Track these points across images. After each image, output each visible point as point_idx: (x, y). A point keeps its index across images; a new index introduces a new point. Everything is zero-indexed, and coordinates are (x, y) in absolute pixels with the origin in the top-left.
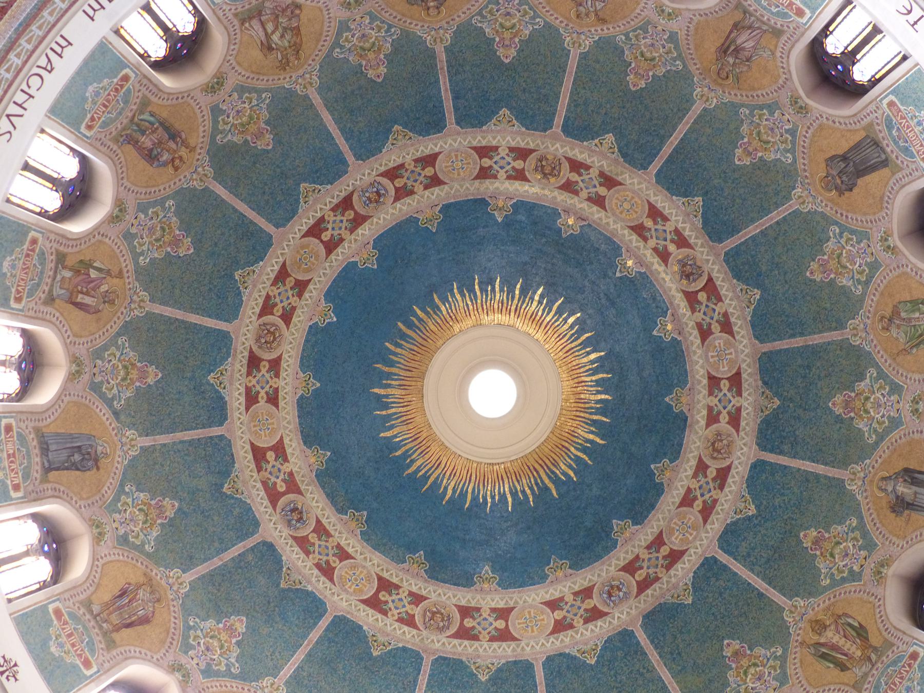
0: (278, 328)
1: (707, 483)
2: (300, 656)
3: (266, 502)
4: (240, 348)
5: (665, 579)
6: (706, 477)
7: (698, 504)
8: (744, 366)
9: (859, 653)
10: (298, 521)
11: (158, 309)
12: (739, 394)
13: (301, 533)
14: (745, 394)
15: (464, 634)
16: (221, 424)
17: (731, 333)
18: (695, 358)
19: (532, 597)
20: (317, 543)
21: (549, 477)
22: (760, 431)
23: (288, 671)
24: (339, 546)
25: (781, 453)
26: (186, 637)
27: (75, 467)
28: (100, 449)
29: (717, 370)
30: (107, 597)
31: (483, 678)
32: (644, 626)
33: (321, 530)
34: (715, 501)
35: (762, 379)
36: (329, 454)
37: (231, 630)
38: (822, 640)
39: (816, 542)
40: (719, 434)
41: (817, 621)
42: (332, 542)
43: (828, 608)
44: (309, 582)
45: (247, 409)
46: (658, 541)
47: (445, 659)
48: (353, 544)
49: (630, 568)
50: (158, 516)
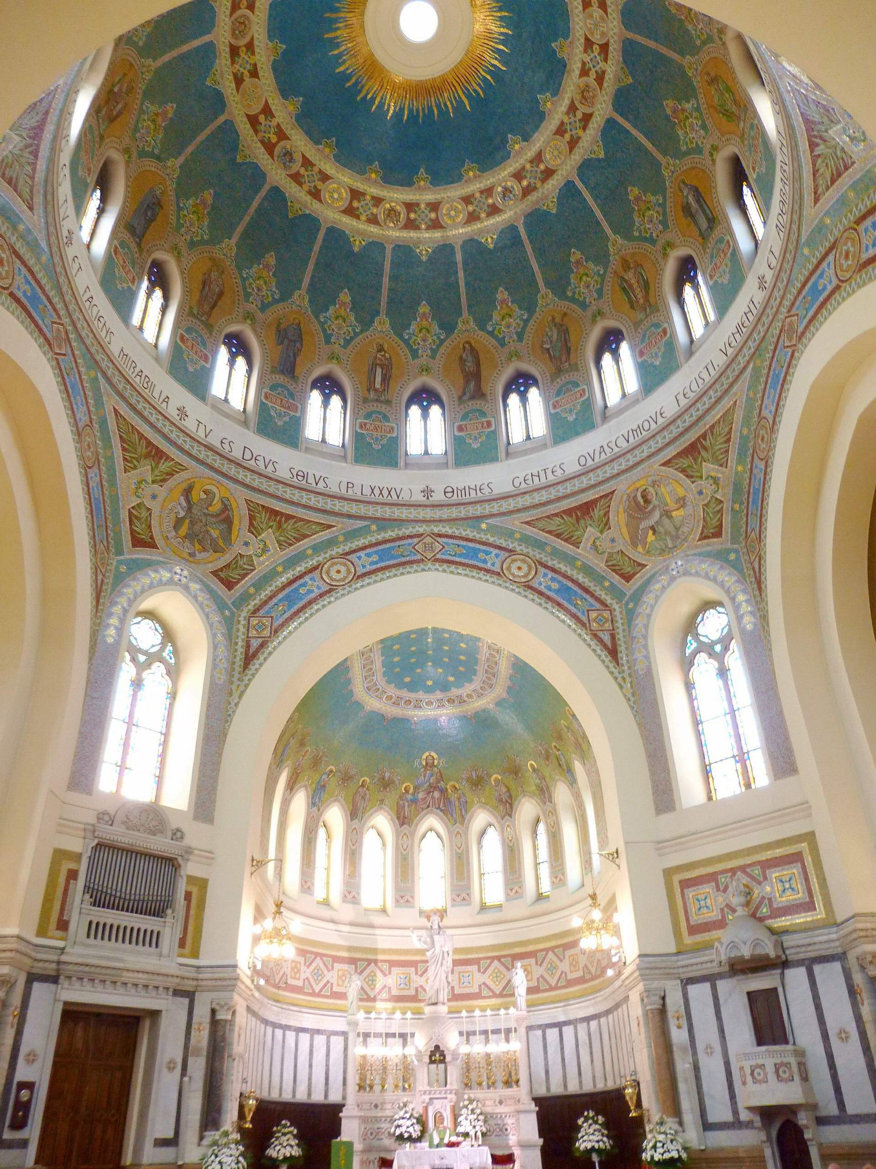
0: (248, 18)
1: (575, 122)
2: (311, 266)
3: (267, 156)
4: (222, 47)
5: (540, 190)
6: (575, 116)
7: (567, 136)
8: (611, 41)
9: (641, 301)
10: (290, 162)
11: (160, 62)
12: (606, 60)
13: (293, 171)
14: (609, 62)
15: (411, 225)
16: (223, 112)
17: (606, 12)
18: (577, 19)
19: (452, 193)
20: (306, 174)
21: (464, 93)
22: (616, 95)
23: (306, 280)
24: (320, 172)
25: (627, 119)
26: (245, 288)
27: (152, 221)
28: (158, 193)
29: (592, 34)
30: (196, 296)
31: (424, 258)
32: (526, 224)
33: (307, 163)
34: (579, 138)
35: (623, 57)
36: (301, 99)
37: (267, 266)
38: (626, 277)
39: (638, 199)
40: (587, 86)
41: (626, 261)
42: (316, 169)
43: (633, 254)
44: (306, 207)
45: (238, 90)
46: (538, 158)
47: (399, 246)
48: (329, 168)
49: (518, 176)
50: (205, 208)
